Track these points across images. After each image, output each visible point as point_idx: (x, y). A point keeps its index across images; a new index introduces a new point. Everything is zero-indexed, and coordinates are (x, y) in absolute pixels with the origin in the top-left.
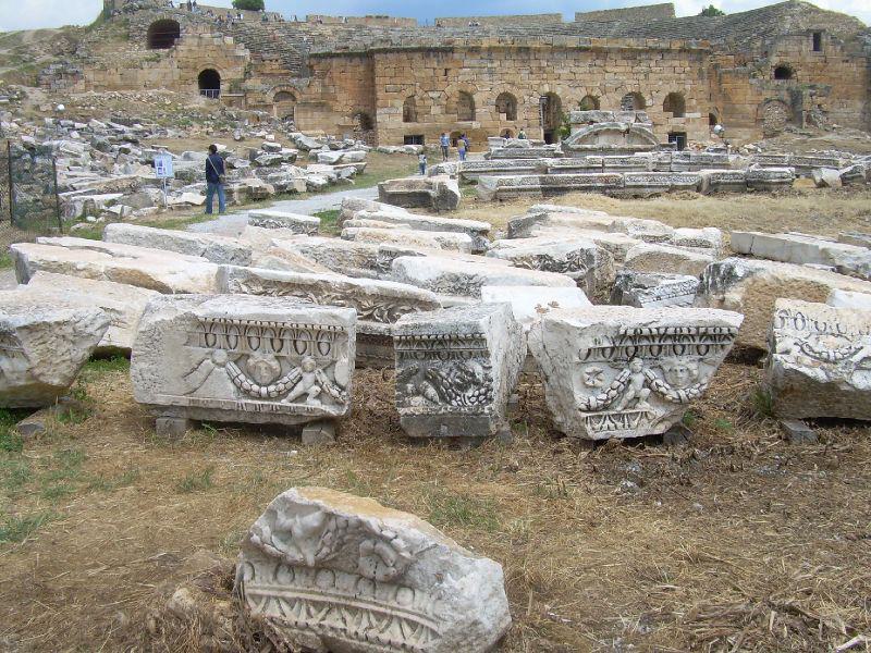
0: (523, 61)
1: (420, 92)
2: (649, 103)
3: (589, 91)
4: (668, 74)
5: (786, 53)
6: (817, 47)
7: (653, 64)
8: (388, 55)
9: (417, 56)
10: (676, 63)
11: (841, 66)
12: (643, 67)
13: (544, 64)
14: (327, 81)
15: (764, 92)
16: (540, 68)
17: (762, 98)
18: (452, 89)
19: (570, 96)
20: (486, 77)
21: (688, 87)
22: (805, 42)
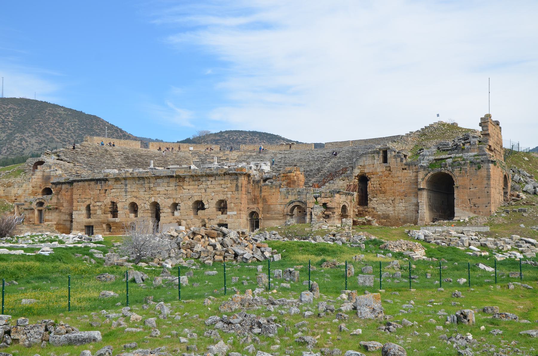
0: (142, 184)
1: (93, 202)
2: (206, 206)
3: (175, 200)
4: (218, 188)
5: (364, 166)
6: (385, 160)
7: (209, 183)
8: (79, 183)
9: (92, 183)
10: (222, 182)
11: (400, 173)
12: (203, 186)
13: (152, 185)
14: (59, 196)
15: (290, 197)
16: (150, 188)
17: (288, 201)
18: (108, 201)
19: (165, 203)
20: (124, 194)
21: (229, 196)
22: (376, 158)
